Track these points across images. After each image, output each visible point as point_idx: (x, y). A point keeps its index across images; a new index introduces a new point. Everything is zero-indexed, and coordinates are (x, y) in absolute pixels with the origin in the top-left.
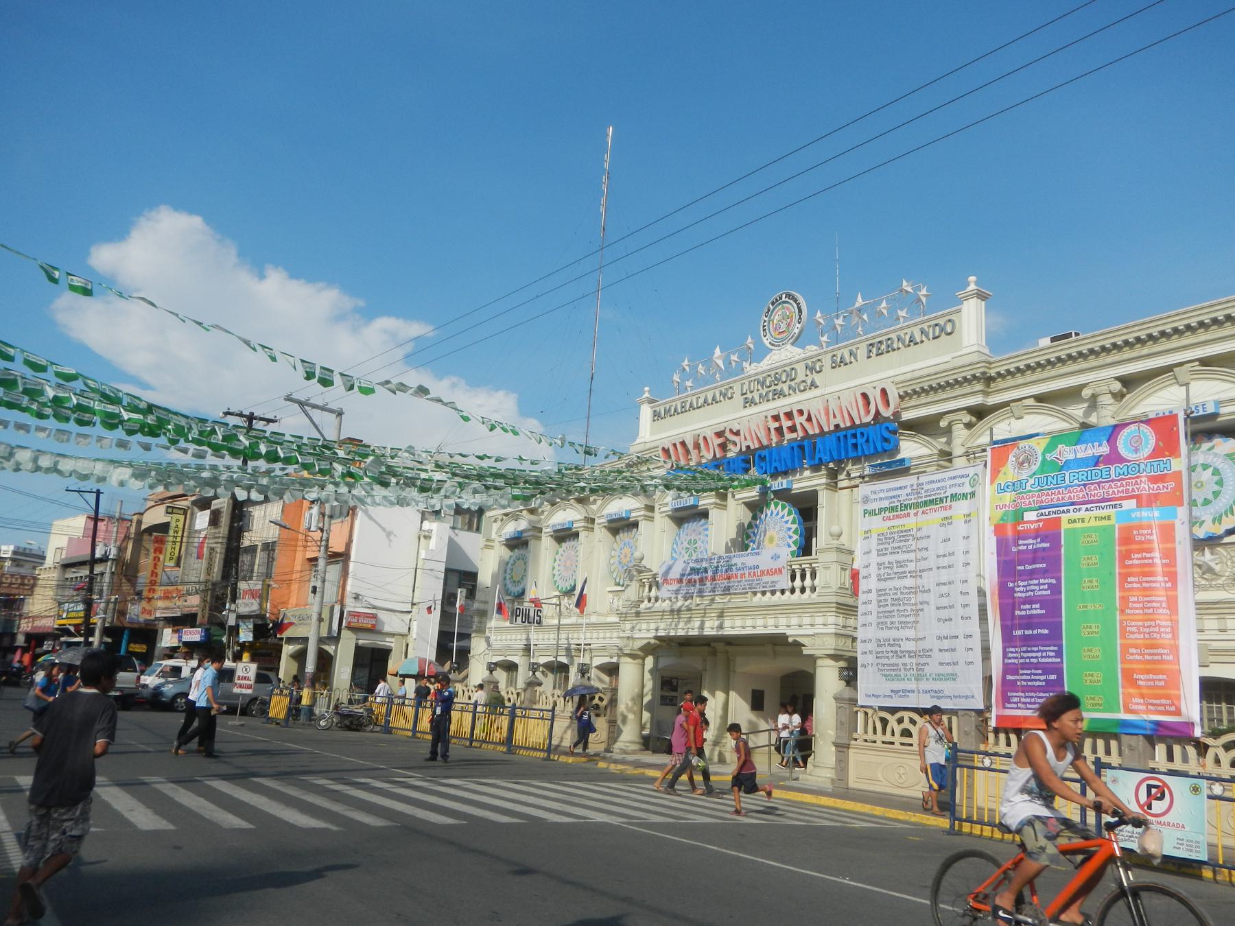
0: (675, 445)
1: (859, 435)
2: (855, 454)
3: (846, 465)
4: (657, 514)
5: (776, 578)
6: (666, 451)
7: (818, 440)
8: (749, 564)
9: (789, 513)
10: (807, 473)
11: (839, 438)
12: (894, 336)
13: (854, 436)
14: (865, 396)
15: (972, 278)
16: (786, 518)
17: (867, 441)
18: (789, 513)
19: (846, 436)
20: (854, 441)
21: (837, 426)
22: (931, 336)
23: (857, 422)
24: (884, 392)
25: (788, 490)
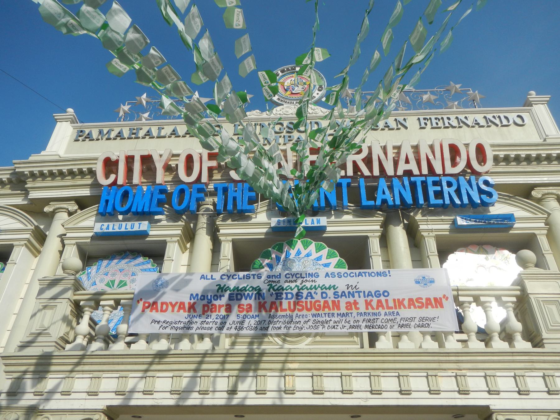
0: (130, 160)
1: (444, 184)
2: (440, 202)
3: (416, 214)
4: (53, 243)
5: (429, 312)
6: (110, 165)
7: (383, 184)
8: (361, 288)
9: (330, 256)
10: (346, 217)
11: (413, 186)
12: (453, 117)
13: (435, 183)
14: (454, 150)
15: (533, 92)
16: (324, 261)
17: (458, 192)
18: (330, 256)
19: (424, 185)
20: (439, 188)
21: (408, 173)
22: (500, 125)
23: (438, 170)
24: (480, 149)
25: (322, 229)
